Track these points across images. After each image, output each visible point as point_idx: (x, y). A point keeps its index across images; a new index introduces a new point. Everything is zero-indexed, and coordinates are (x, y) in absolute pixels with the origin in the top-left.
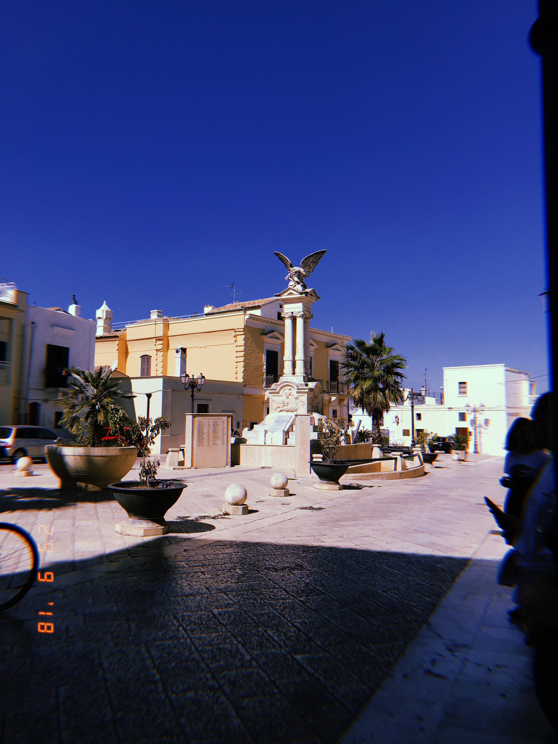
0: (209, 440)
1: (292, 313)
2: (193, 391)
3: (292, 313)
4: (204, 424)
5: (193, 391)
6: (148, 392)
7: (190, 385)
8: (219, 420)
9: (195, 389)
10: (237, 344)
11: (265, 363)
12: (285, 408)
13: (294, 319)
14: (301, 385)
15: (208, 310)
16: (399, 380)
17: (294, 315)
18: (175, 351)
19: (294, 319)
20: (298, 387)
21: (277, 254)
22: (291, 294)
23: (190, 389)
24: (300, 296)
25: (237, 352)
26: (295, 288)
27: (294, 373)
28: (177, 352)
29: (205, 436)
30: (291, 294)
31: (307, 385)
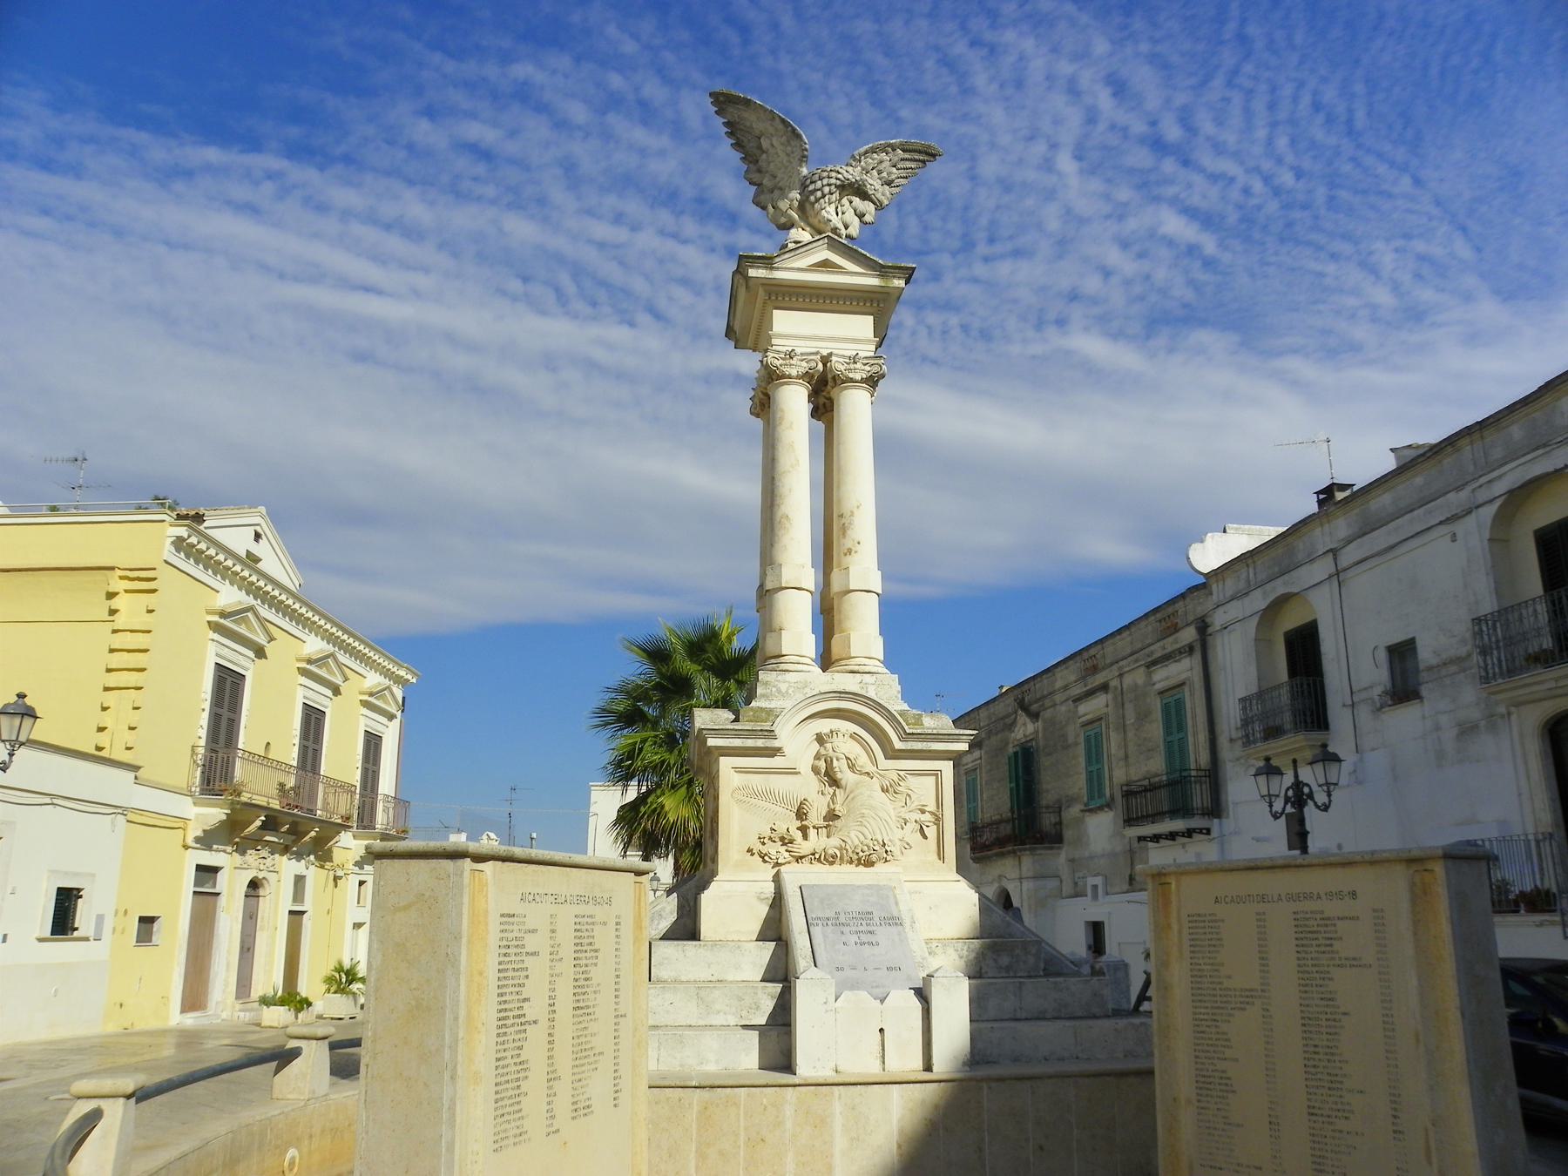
0: (553, 1078)
3: (825, 360)
4: (531, 943)
8: (599, 913)
10: (121, 621)
11: (207, 705)
12: (816, 841)
13: (824, 392)
17: (838, 365)
19: (824, 392)
22: (825, 265)
24: (873, 281)
25: (112, 651)
27: (826, 661)
29: (534, 1048)
30: (825, 265)
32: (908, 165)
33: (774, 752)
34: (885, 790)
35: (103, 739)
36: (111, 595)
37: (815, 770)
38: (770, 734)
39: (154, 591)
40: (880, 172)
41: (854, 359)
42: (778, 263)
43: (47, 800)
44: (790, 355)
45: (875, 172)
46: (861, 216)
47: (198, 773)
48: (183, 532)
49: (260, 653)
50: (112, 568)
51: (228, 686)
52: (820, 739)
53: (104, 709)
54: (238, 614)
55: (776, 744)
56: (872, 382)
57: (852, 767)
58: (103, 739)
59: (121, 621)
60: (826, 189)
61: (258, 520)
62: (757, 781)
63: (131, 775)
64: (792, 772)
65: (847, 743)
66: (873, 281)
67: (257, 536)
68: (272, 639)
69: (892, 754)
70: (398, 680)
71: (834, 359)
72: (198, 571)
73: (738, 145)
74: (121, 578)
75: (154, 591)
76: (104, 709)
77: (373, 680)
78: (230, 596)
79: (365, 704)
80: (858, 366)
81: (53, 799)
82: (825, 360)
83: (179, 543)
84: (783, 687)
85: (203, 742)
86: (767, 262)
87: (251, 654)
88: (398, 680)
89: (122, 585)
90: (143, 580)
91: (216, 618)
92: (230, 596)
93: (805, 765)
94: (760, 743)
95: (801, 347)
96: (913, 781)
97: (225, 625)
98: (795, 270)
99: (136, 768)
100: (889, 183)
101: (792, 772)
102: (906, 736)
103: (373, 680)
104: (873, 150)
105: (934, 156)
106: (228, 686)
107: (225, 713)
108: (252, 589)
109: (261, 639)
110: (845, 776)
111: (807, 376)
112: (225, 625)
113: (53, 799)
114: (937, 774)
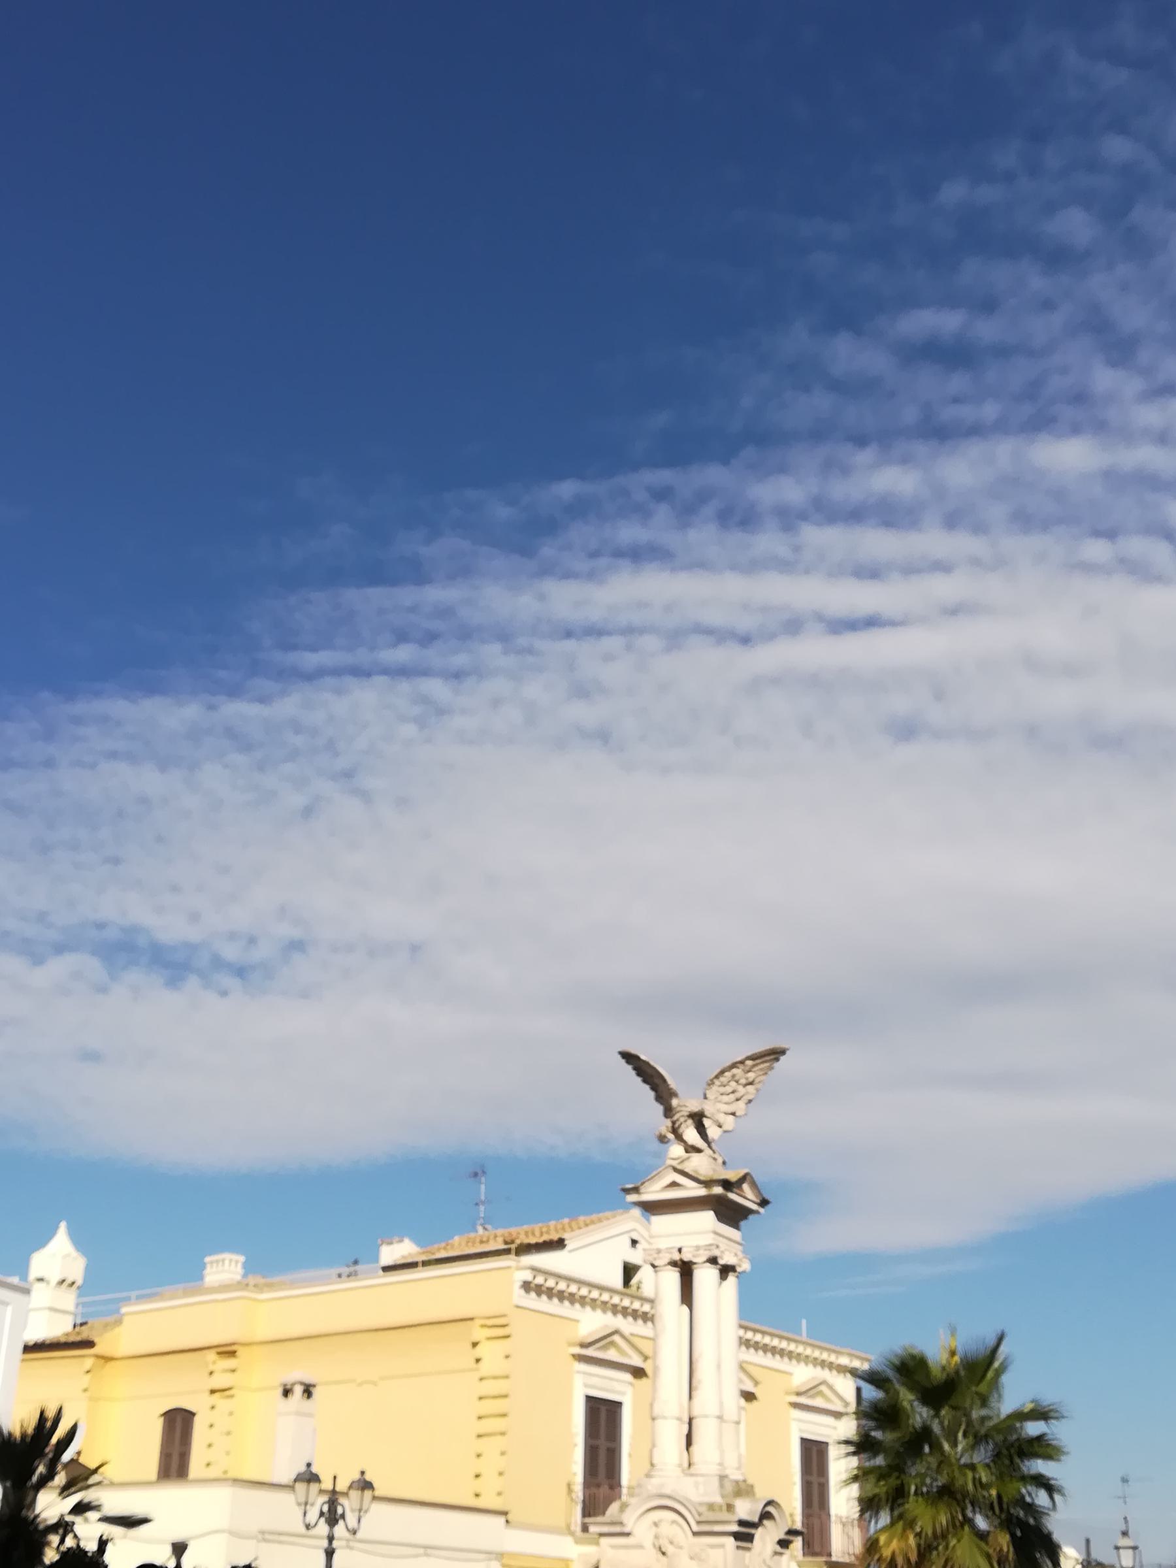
1: (680, 1250)
2: (331, 1539)
5: (331, 1539)
6: (178, 1537)
7: (322, 1514)
9: (340, 1530)
10: (486, 1368)
13: (686, 1270)
14: (711, 1507)
15: (390, 1254)
16: (1041, 1498)
17: (687, 1257)
18: (280, 1391)
19: (686, 1270)
20: (700, 1515)
21: (629, 1057)
22: (674, 1184)
23: (323, 1528)
26: (688, 1167)
28: (287, 1392)
30: (674, 1184)
31: (730, 1508)
32: (762, 1066)
33: (628, 1534)
34: (692, 1558)
35: (478, 1485)
36: (475, 1345)
37: (654, 1546)
38: (621, 1523)
39: (508, 1337)
40: (737, 1082)
41: (698, 1248)
42: (642, 1190)
43: (422, 1551)
44: (659, 1251)
45: (733, 1084)
46: (733, 1114)
47: (578, 1510)
48: (527, 1276)
49: (639, 1373)
50: (472, 1319)
51: (603, 1417)
52: (656, 1524)
53: (479, 1456)
54: (606, 1339)
55: (626, 1530)
56: (713, 1261)
57: (671, 1543)
58: (478, 1485)
59: (486, 1368)
60: (682, 1120)
61: (631, 1225)
62: (622, 1553)
63: (502, 1519)
64: (640, 1547)
65: (672, 1528)
66: (702, 1192)
67: (634, 1242)
68: (646, 1358)
69: (695, 1534)
70: (842, 1369)
71: (684, 1250)
72: (554, 1306)
73: (645, 1081)
74: (483, 1326)
75: (508, 1337)
76: (479, 1456)
77: (803, 1374)
78: (591, 1323)
79: (795, 1405)
80: (701, 1252)
81: (428, 1549)
82: (680, 1250)
83: (527, 1286)
84: (650, 1487)
85: (579, 1478)
86: (636, 1190)
87: (628, 1377)
88: (842, 1369)
89: (479, 1334)
90: (500, 1328)
91: (578, 1350)
92: (591, 1323)
93: (648, 1542)
94: (617, 1529)
95: (663, 1244)
96: (711, 1552)
97: (590, 1354)
98: (654, 1192)
99: (505, 1513)
100: (751, 1083)
101: (640, 1547)
102: (698, 1523)
103: (803, 1374)
104: (722, 1072)
105: (783, 1052)
106: (603, 1417)
107: (602, 1443)
108: (615, 1309)
109: (636, 1361)
110: (670, 1549)
111: (674, 1264)
112: (590, 1354)
113: (428, 1549)
114: (722, 1546)
